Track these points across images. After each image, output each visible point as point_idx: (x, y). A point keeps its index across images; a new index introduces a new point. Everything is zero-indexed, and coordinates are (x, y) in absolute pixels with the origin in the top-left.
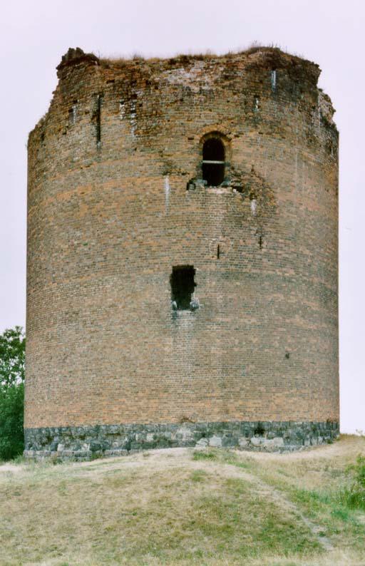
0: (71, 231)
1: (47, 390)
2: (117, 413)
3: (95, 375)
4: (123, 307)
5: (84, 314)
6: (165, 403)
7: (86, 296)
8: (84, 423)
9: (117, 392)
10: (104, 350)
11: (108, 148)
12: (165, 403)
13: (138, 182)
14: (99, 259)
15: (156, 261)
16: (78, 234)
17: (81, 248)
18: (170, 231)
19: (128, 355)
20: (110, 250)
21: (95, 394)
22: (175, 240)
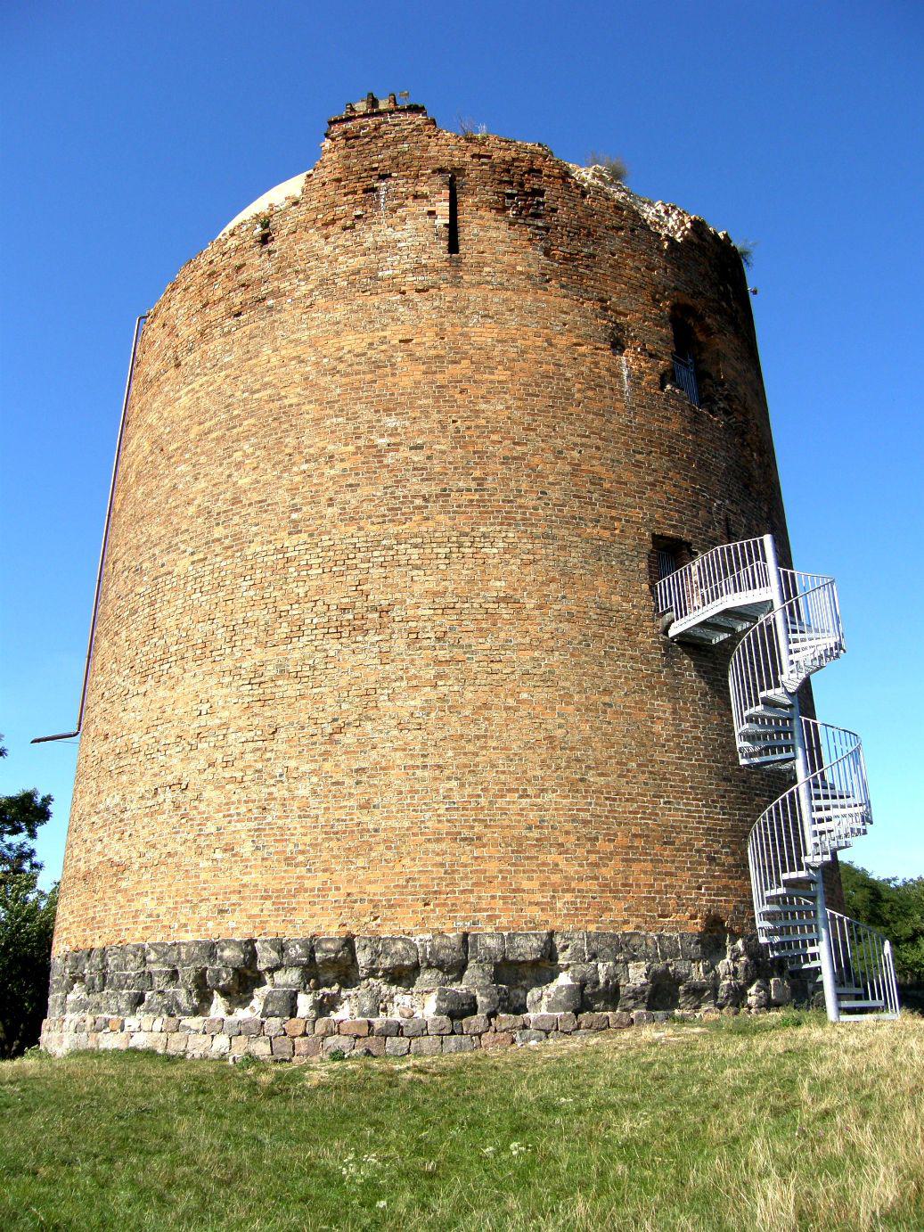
0: (368, 415)
1: (252, 825)
2: (538, 897)
3: (454, 783)
4: (540, 607)
5: (411, 612)
6: (671, 874)
7: (417, 568)
8: (417, 929)
9: (535, 834)
10: (486, 713)
11: (480, 266)
12: (671, 874)
13: (562, 342)
14: (461, 484)
15: (614, 513)
16: (391, 422)
17: (400, 455)
18: (638, 457)
19: (560, 733)
20: (495, 466)
21: (454, 837)
22: (651, 479)
